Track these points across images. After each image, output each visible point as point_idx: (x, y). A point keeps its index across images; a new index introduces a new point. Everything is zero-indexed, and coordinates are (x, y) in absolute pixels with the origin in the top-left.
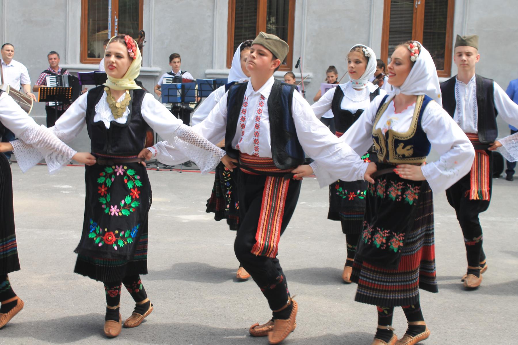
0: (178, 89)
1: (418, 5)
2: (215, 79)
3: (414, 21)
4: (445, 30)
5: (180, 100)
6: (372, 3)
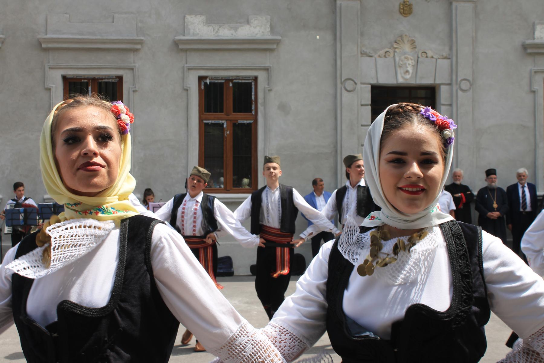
0: (21, 213)
1: (227, 134)
2: (55, 203)
3: (224, 147)
4: (251, 154)
5: (23, 223)
6: (189, 134)
